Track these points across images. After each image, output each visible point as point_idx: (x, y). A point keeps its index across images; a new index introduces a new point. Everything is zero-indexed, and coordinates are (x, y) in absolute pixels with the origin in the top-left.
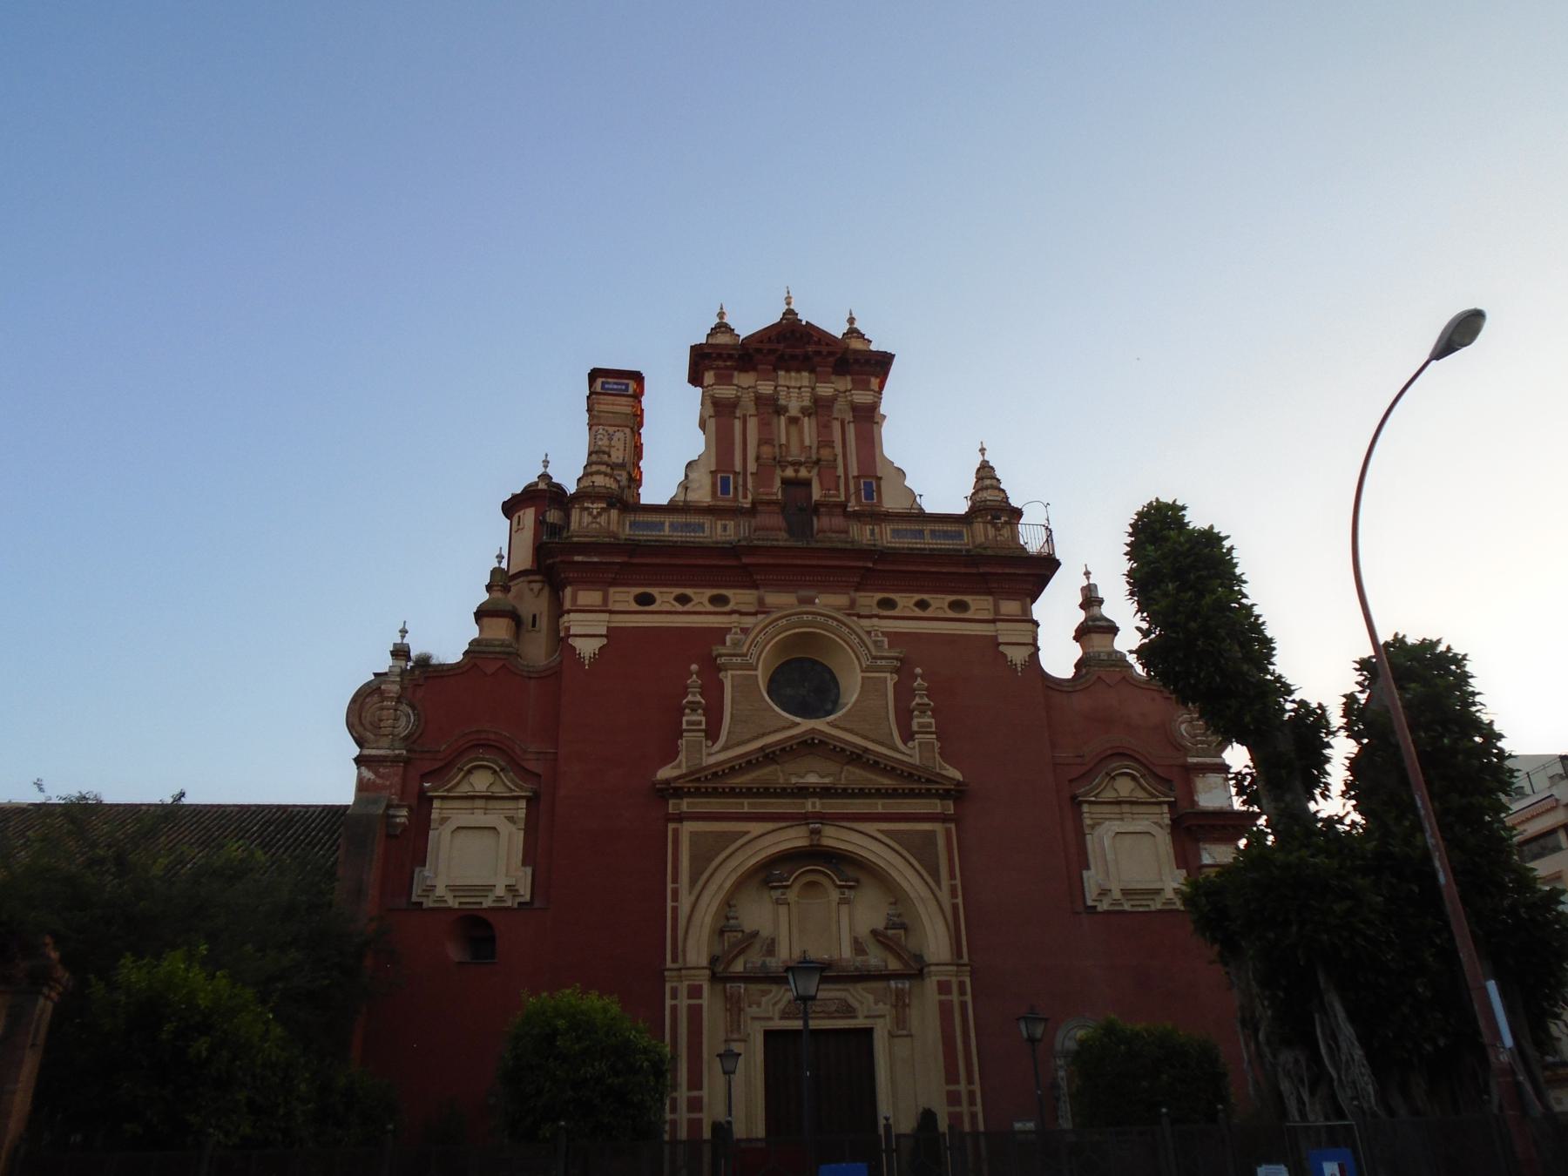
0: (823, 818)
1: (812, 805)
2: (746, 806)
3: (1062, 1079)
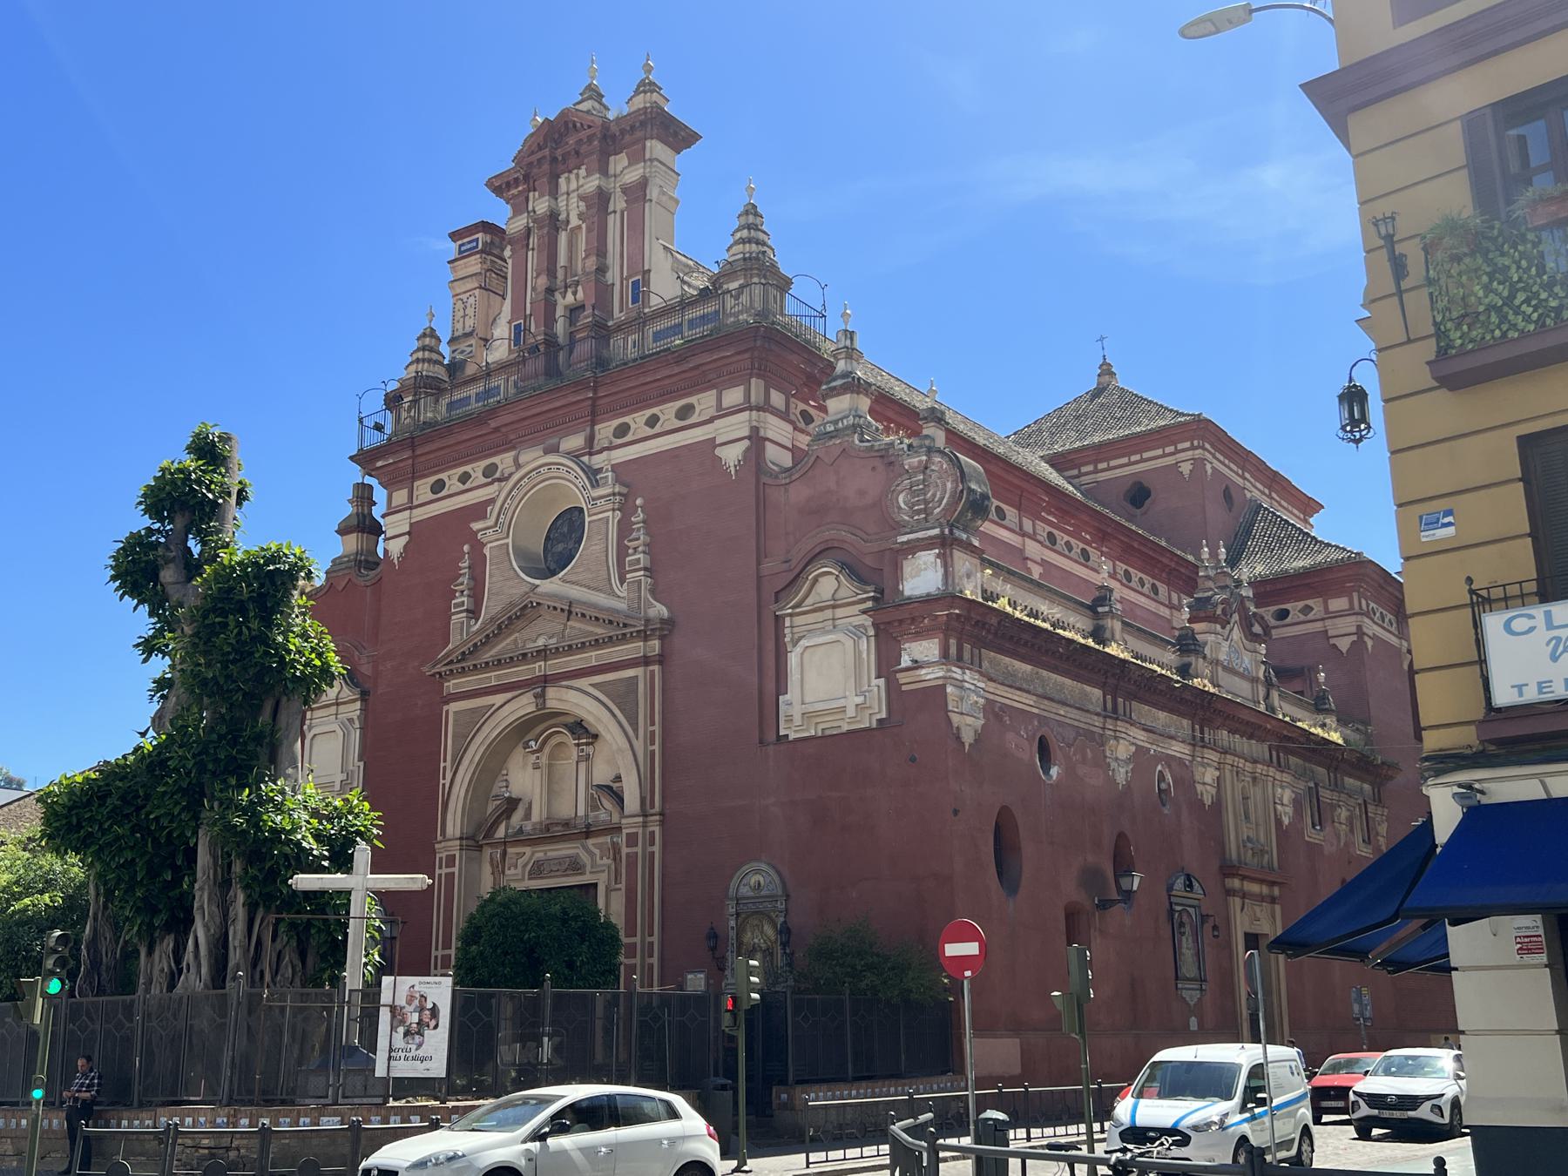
0: (546, 681)
1: (539, 668)
2: (493, 678)
3: (733, 928)
